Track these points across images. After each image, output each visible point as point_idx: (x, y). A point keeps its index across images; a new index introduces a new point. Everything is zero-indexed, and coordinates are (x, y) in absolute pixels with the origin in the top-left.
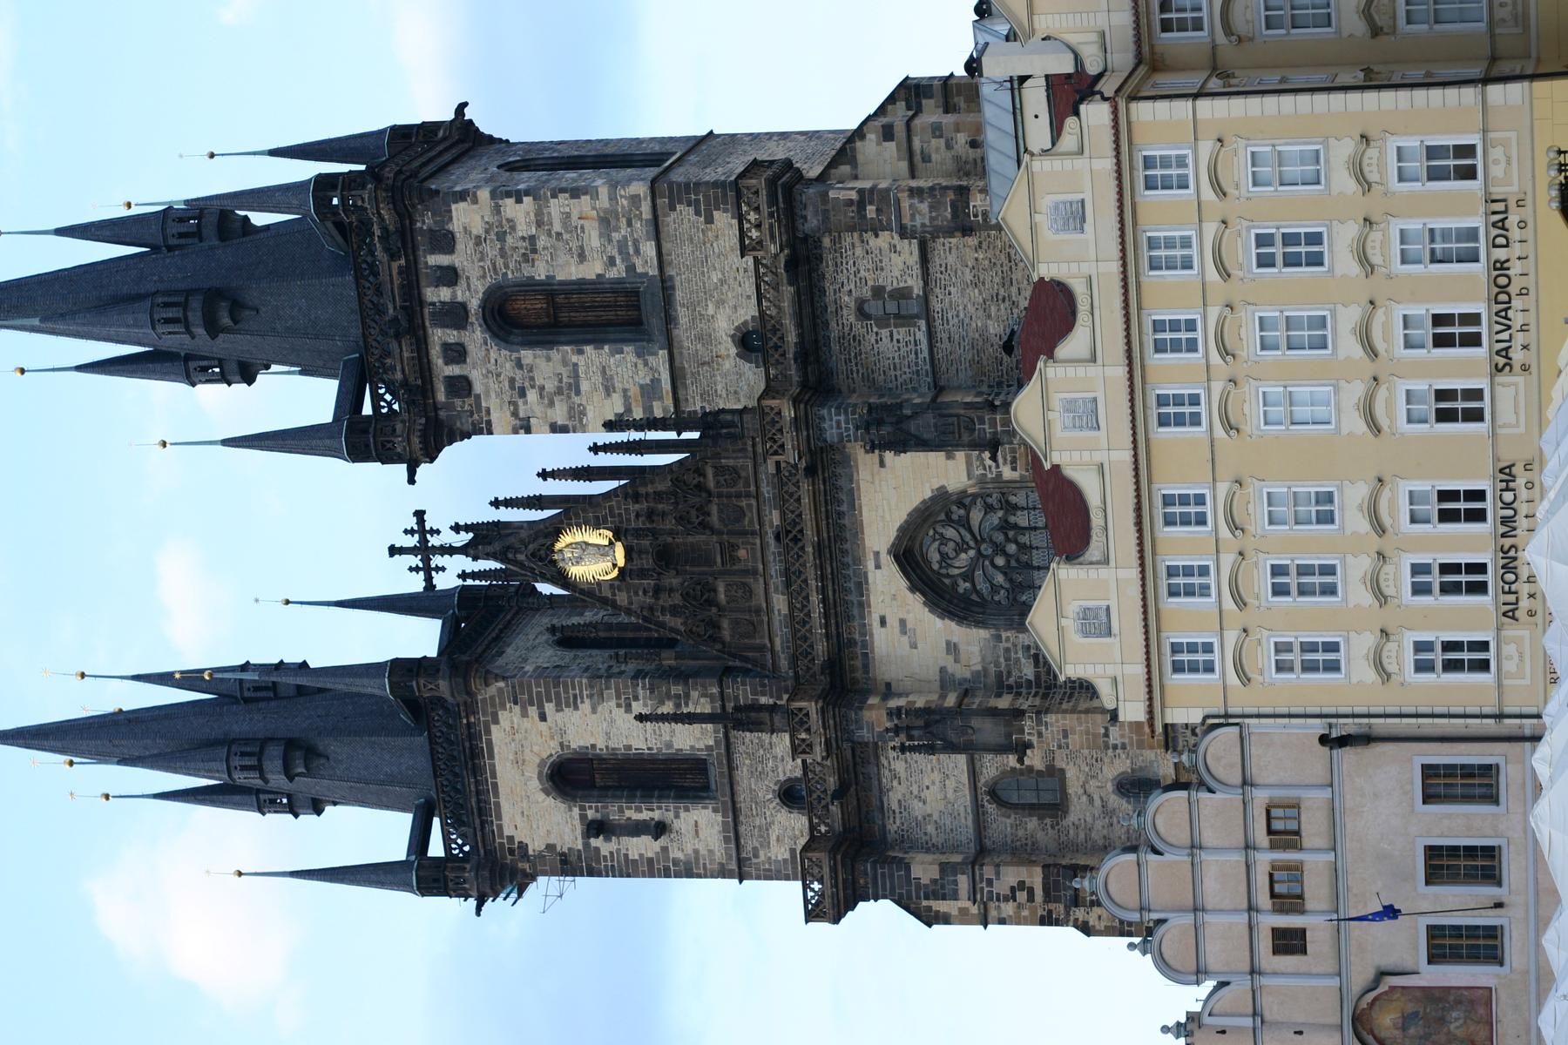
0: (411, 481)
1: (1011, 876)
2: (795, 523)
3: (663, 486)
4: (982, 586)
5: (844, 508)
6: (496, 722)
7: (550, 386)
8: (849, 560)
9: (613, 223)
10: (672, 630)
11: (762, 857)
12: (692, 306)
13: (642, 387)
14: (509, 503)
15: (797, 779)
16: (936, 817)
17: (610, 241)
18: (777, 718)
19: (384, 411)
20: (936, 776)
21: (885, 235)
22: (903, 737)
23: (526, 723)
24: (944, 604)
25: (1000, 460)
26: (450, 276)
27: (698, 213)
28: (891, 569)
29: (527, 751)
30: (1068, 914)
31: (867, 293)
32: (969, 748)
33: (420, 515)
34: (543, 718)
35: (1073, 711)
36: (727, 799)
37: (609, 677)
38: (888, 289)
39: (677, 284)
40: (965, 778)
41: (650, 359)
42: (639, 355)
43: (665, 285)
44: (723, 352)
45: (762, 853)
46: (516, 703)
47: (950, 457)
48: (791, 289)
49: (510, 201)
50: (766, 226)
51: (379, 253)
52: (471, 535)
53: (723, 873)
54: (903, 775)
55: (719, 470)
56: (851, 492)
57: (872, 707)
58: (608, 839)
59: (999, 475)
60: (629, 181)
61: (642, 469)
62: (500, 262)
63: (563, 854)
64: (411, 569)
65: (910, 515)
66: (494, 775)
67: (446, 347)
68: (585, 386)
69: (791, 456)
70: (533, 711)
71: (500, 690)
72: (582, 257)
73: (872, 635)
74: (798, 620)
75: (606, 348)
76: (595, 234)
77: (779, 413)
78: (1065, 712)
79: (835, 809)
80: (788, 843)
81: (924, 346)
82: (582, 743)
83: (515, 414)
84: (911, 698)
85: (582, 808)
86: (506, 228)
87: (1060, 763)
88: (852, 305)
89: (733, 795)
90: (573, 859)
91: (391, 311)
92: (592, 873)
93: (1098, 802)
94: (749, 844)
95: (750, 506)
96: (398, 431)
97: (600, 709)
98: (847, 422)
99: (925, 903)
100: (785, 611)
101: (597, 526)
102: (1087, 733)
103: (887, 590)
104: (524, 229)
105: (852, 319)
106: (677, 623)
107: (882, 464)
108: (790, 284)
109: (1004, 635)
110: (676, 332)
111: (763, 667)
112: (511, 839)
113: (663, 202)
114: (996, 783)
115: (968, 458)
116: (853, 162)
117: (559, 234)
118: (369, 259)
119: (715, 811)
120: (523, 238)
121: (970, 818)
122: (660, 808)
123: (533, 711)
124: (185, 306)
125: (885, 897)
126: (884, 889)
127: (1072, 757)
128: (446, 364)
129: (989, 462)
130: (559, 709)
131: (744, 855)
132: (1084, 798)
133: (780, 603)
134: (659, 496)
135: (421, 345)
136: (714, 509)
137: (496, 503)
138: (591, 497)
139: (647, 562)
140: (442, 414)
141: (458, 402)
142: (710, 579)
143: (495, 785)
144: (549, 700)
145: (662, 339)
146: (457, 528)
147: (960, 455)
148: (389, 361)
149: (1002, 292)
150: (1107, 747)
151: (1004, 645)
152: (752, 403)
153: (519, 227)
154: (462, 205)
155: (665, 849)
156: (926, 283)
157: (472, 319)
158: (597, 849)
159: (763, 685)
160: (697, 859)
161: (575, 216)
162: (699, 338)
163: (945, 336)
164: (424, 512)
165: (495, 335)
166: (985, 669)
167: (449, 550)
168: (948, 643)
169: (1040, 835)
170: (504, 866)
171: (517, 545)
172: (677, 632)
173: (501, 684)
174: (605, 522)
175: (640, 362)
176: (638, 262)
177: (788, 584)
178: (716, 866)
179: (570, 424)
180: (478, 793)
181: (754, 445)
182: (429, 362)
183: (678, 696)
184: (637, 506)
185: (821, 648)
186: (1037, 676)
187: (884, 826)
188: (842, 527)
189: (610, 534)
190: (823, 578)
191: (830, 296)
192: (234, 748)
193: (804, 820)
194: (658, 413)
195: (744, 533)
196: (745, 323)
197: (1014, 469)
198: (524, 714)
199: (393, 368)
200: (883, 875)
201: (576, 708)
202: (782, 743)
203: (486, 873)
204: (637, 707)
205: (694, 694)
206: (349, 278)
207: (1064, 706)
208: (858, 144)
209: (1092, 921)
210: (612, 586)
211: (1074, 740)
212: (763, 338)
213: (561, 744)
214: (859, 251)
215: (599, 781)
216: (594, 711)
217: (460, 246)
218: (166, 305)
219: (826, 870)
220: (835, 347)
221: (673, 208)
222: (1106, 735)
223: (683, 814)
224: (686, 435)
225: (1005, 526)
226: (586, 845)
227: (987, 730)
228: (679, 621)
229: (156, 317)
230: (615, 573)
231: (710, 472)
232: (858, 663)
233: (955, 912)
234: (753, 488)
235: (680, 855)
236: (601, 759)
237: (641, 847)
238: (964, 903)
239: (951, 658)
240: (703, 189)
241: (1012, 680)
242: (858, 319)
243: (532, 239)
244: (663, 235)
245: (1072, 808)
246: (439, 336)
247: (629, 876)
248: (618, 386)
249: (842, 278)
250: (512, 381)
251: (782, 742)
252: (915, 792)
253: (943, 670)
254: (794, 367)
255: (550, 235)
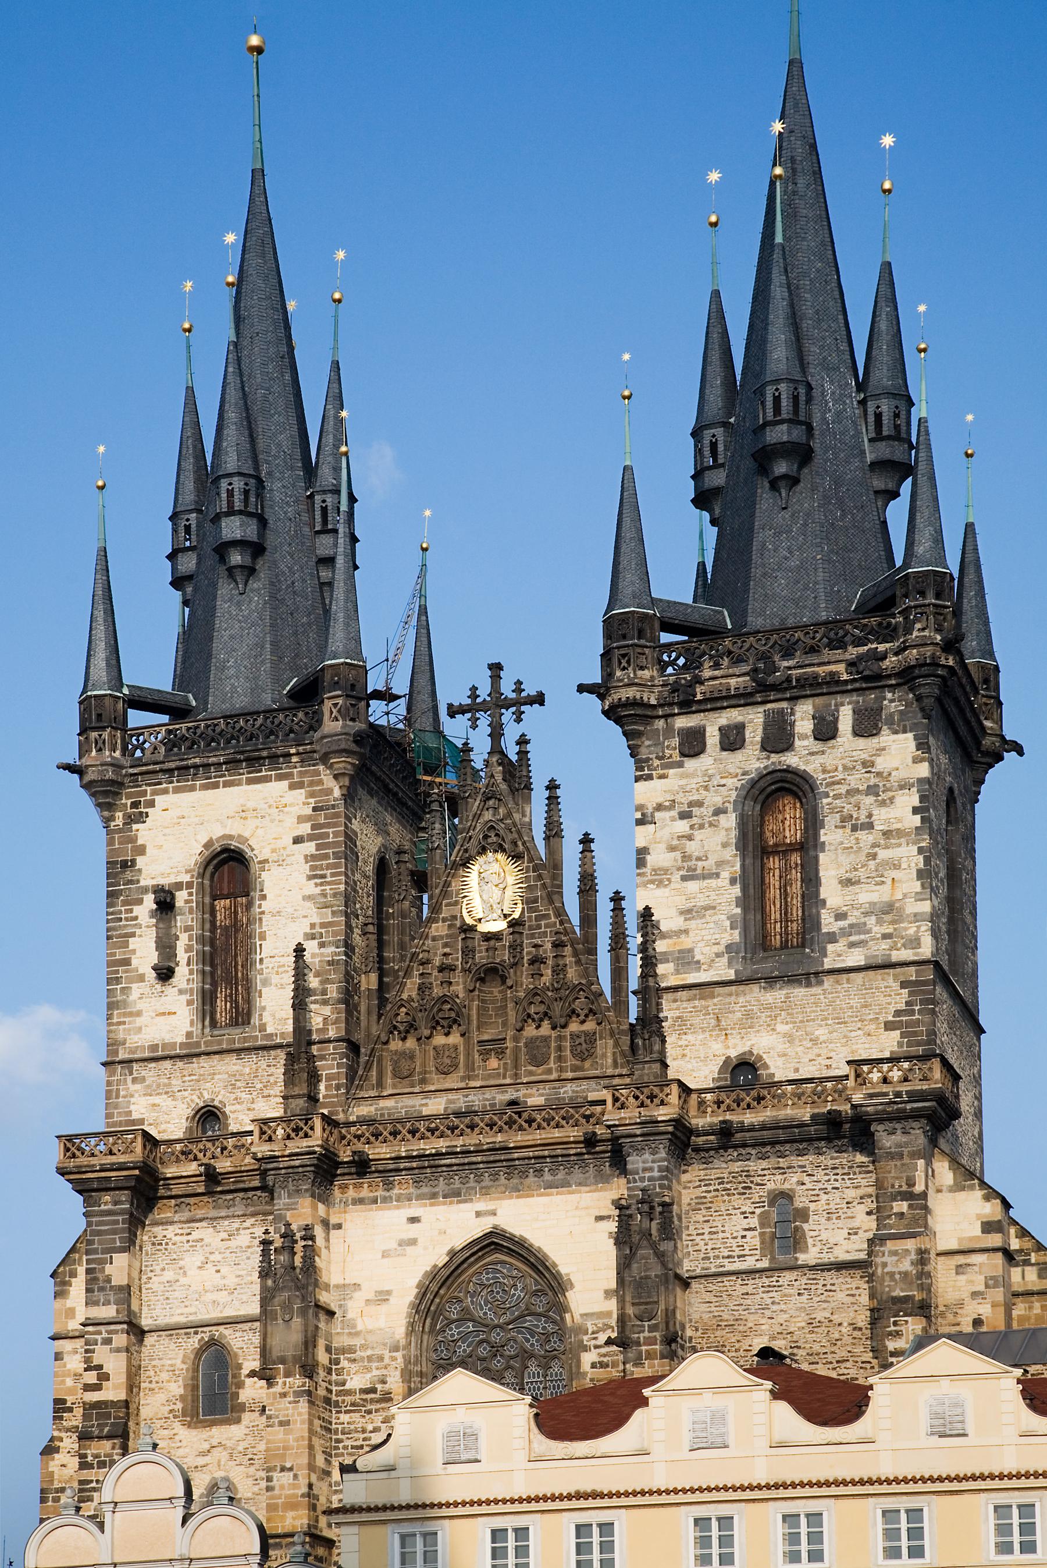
0: (582, 688)
1: (115, 1365)
2: (530, 1121)
3: (572, 974)
4: (454, 1331)
5: (547, 1177)
6: (292, 787)
7: (692, 847)
8: (487, 1181)
9: (888, 918)
10: (403, 985)
11: (133, 1088)
12: (787, 1006)
13: (690, 951)
14: (553, 800)
15: (227, 1125)
16: (183, 1280)
17: (866, 914)
18: (301, 1102)
19: (665, 657)
20: (231, 1281)
21: (871, 1223)
22: (278, 1243)
23: (290, 821)
24: (434, 1287)
25: (603, 1350)
26: (825, 731)
27: (898, 1013)
28: (478, 1228)
29: (258, 822)
30: (68, 1430)
31: (799, 1202)
32: (266, 1316)
33: (539, 699)
34: (297, 840)
35: (311, 1432)
36: (203, 1048)
37: (347, 915)
38: (805, 1226)
39: (814, 990)
40: (230, 1312)
41: (725, 960)
42: (729, 948)
43: (812, 977)
44: (731, 1041)
45: (138, 1087)
46: (315, 809)
47: (608, 1294)
48: (807, 1118)
49: (915, 801)
50: (885, 1088)
51: (853, 652)
52: (514, 758)
53: (113, 1045)
54: (233, 1244)
55: (591, 1039)
56: (565, 1184)
57: (315, 1208)
58: (153, 914)
59: (586, 1349)
60: (935, 934)
61: (593, 951)
62: (842, 789)
63: (133, 861)
64: (474, 689)
65: (539, 1250)
66: (226, 784)
67: (740, 728)
68: (693, 886)
69: (612, 1116)
70: (306, 829)
71: (329, 792)
72: (847, 882)
73: (398, 1208)
74: (414, 1126)
75: (739, 910)
76: (874, 897)
77: (662, 1103)
78: (311, 1423)
79: (193, 1168)
80: (149, 1116)
81: (738, 1266)
82: (266, 885)
83: (659, 807)
84: (324, 1252)
85: (189, 885)
86: (883, 796)
87: (247, 1417)
88: (787, 1186)
89: (208, 1054)
90: (128, 875)
91: (785, 664)
92: (111, 895)
93: (201, 1461)
94: (149, 1072)
95: (549, 1071)
96: (640, 673)
97: (309, 904)
98: (650, 1179)
99: (81, 1270)
100: (425, 1111)
101: (529, 902)
102: (285, 1448)
103: (452, 1223)
104: (882, 817)
105: (770, 1186)
106: (410, 989)
107: (600, 1218)
108: (814, 1117)
109: (399, 1355)
110: (755, 988)
111: (360, 1087)
112: (151, 804)
113: (911, 973)
114: (223, 1346)
115: (609, 1314)
116: (957, 1187)
117: (874, 856)
118: (848, 638)
119: (189, 1035)
120: (870, 816)
121: (183, 1320)
122: (191, 972)
123: (306, 829)
124: (793, 422)
125: (89, 1224)
126: (98, 1224)
127: (254, 1431)
128: (720, 729)
129: (602, 1338)
130: (309, 858)
131: (135, 1066)
132: (206, 1446)
133: (436, 1105)
134: (559, 970)
135: (744, 699)
136: (545, 1029)
137: (552, 786)
138: (561, 894)
139: (481, 957)
140: (660, 724)
141: (675, 741)
142: (463, 1028)
143: (216, 786)
144: (318, 847)
145: (747, 973)
146: (523, 741)
147: (612, 1305)
148: (726, 661)
149: (800, 1352)
150: (269, 1470)
151: (387, 1355)
152: (671, 1074)
153: (884, 810)
154: (912, 745)
155: (141, 978)
156: (813, 1268)
157: (774, 758)
158: (140, 902)
159: (338, 1087)
160: (131, 1014)
161: (894, 874)
162: (748, 1015)
163: (749, 1289)
164: (542, 704)
165: (754, 783)
166: (357, 1334)
167: (496, 733)
168: (389, 1293)
169: (161, 1397)
170: (117, 794)
171: (502, 811)
172: (401, 991)
173: (337, 793)
174: (531, 910)
175: (721, 948)
176: (840, 946)
177: (458, 1114)
178: (121, 1036)
179: (648, 870)
180: (206, 766)
181: (621, 1076)
182: (725, 708)
183: (324, 992)
184: (549, 946)
185: (378, 1151)
186: (349, 1393)
187: (172, 1223)
188: (524, 1175)
189: (516, 915)
190: (466, 1153)
191: (796, 1161)
192: (252, 481)
193: (179, 1134)
194: (661, 969)
195: (516, 1066)
196: (766, 1066)
197: (593, 1366)
198: (301, 819)
199: (717, 666)
200: (117, 1222)
201: (310, 878)
202: (273, 1108)
203: (110, 775)
204: (311, 947)
205: (327, 1010)
206: (823, 616)
207: (317, 1423)
208: (979, 1194)
209: (59, 1458)
210: (454, 917)
211: (278, 1433)
212: (748, 1086)
213: (266, 861)
214: (851, 1194)
215: (220, 904)
216: (308, 898)
217: (862, 742)
218: (796, 399)
219: (122, 1159)
220: (737, 1166)
221: (904, 985)
222: (283, 1469)
223: (184, 998)
224: (633, 1002)
225: (526, 1355)
226: (145, 890)
227: (288, 1337)
228: (414, 994)
229: (783, 387)
230: (469, 921)
231: (590, 1026)
232: (365, 1193)
233: (69, 1303)
234: (570, 1075)
235: (134, 995)
236: (249, 905)
237: (144, 952)
238: (82, 1313)
239: (371, 1296)
240: (927, 1018)
241: (344, 1363)
242: (770, 1192)
243: (870, 826)
244: (871, 973)
245: (194, 1432)
246: (754, 720)
247: (108, 938)
248: (692, 924)
249: (820, 1174)
250: (700, 804)
251: (273, 1108)
252: (212, 1258)
253: (357, 1286)
254: (716, 1120)
255: (874, 845)
